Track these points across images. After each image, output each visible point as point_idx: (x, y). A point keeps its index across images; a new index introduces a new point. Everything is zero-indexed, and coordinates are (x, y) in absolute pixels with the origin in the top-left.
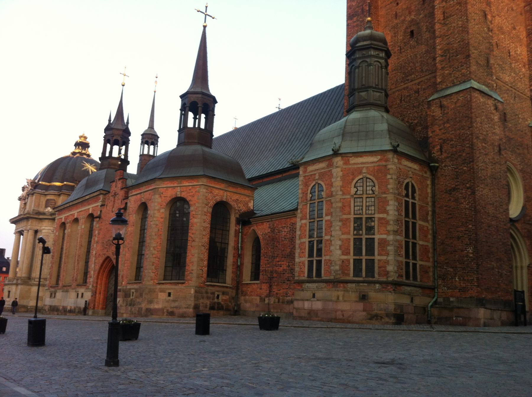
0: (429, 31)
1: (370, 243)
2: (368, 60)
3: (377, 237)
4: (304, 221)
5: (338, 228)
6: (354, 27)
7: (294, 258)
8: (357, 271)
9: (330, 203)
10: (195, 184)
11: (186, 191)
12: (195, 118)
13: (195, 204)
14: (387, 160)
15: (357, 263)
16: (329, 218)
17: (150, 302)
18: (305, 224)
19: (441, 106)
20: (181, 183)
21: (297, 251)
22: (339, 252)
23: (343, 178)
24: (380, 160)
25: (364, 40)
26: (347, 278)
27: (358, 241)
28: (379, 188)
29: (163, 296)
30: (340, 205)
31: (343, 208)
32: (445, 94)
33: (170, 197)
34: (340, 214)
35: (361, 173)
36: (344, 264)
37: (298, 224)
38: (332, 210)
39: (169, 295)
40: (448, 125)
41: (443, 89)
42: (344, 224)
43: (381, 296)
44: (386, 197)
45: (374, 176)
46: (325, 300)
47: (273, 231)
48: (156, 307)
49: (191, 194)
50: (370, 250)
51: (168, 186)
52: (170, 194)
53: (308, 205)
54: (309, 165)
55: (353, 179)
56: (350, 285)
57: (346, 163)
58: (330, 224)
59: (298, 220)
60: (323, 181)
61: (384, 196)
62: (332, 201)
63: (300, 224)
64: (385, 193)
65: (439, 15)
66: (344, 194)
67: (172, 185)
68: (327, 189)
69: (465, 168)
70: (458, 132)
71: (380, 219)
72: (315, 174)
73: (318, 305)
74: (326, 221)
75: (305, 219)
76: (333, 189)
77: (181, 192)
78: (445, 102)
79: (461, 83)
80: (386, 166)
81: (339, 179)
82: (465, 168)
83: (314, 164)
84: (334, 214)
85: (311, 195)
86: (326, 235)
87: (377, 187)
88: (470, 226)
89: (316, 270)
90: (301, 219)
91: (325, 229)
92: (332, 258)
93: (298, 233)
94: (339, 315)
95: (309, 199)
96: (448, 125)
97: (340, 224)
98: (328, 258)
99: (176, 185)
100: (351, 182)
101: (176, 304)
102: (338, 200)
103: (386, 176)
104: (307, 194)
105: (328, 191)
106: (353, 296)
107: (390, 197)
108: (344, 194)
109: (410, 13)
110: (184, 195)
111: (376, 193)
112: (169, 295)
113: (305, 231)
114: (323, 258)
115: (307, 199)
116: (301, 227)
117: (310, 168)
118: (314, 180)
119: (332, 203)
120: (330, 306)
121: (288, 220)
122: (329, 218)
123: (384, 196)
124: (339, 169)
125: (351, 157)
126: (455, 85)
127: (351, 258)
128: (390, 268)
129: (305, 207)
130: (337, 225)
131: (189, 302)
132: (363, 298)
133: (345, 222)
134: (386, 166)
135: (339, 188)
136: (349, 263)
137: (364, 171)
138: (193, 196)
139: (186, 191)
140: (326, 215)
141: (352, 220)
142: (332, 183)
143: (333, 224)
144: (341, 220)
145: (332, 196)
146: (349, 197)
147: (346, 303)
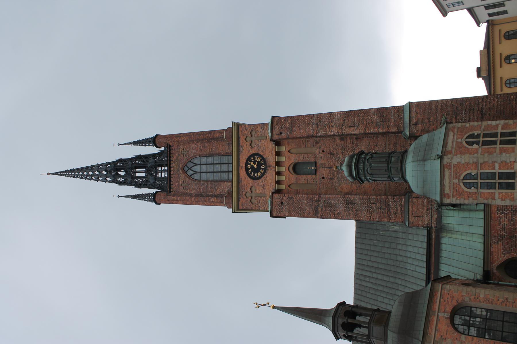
0: (355, 149)
4: (497, 196)
5: (508, 155)
6: (325, 210)
9: (484, 164)
10: (439, 295)
11: (445, 305)
12: (360, 326)
13: (462, 296)
16: (497, 165)
18: (500, 193)
19: (416, 124)
20: (435, 311)
24: (453, 131)
25: (352, 162)
28: (476, 131)
30: (486, 155)
31: (490, 153)
32: (408, 120)
33: (448, 326)
34: (495, 154)
35: (461, 143)
37: (498, 202)
38: (490, 162)
40: (432, 118)
41: (403, 126)
42: (505, 152)
44: (484, 126)
45: (465, 134)
47: (501, 238)
49: (450, 300)
51: (434, 328)
52: (444, 326)
53: (482, 191)
54: (444, 191)
55: (465, 147)
57: (450, 152)
58: (504, 164)
59: (494, 203)
60: (462, 174)
61: (483, 127)
62: (482, 162)
63: (499, 200)
64: (481, 127)
65: (350, 131)
66: (477, 153)
67: (435, 323)
68: (470, 169)
69: (467, 104)
70: (439, 110)
71: (502, 128)
72: (454, 183)
74: (500, 168)
75: (495, 195)
76: (471, 162)
77: (445, 312)
78: (414, 121)
79: (404, 113)
80: (458, 128)
81: (463, 156)
82: (467, 104)
83: (444, 185)
84: (495, 160)
85: (473, 188)
87: (474, 132)
88: (512, 97)
90: (494, 199)
91: (508, 169)
93: (507, 203)
95: (475, 190)
96: (432, 118)
97: (504, 154)
99: (435, 318)
100: (468, 148)
102: (482, 156)
103: (466, 128)
104: (470, 193)
105: (472, 168)
108: (477, 153)
110: (449, 309)
111: (480, 132)
113: (506, 193)
115: (476, 193)
116: (502, 200)
117: (447, 190)
118: (459, 184)
119: (484, 162)
121: (493, 215)
122: (497, 165)
123: (483, 127)
124: (455, 157)
125: (446, 150)
126: (403, 117)
129: (483, 195)
133: (502, 151)
134: (458, 128)
135: (471, 156)
137: (459, 140)
138: (453, 297)
139: (445, 305)
140: (494, 169)
141: (501, 146)
142: (466, 163)
143: (504, 159)
144: (501, 153)
145: (476, 163)
146: (480, 149)
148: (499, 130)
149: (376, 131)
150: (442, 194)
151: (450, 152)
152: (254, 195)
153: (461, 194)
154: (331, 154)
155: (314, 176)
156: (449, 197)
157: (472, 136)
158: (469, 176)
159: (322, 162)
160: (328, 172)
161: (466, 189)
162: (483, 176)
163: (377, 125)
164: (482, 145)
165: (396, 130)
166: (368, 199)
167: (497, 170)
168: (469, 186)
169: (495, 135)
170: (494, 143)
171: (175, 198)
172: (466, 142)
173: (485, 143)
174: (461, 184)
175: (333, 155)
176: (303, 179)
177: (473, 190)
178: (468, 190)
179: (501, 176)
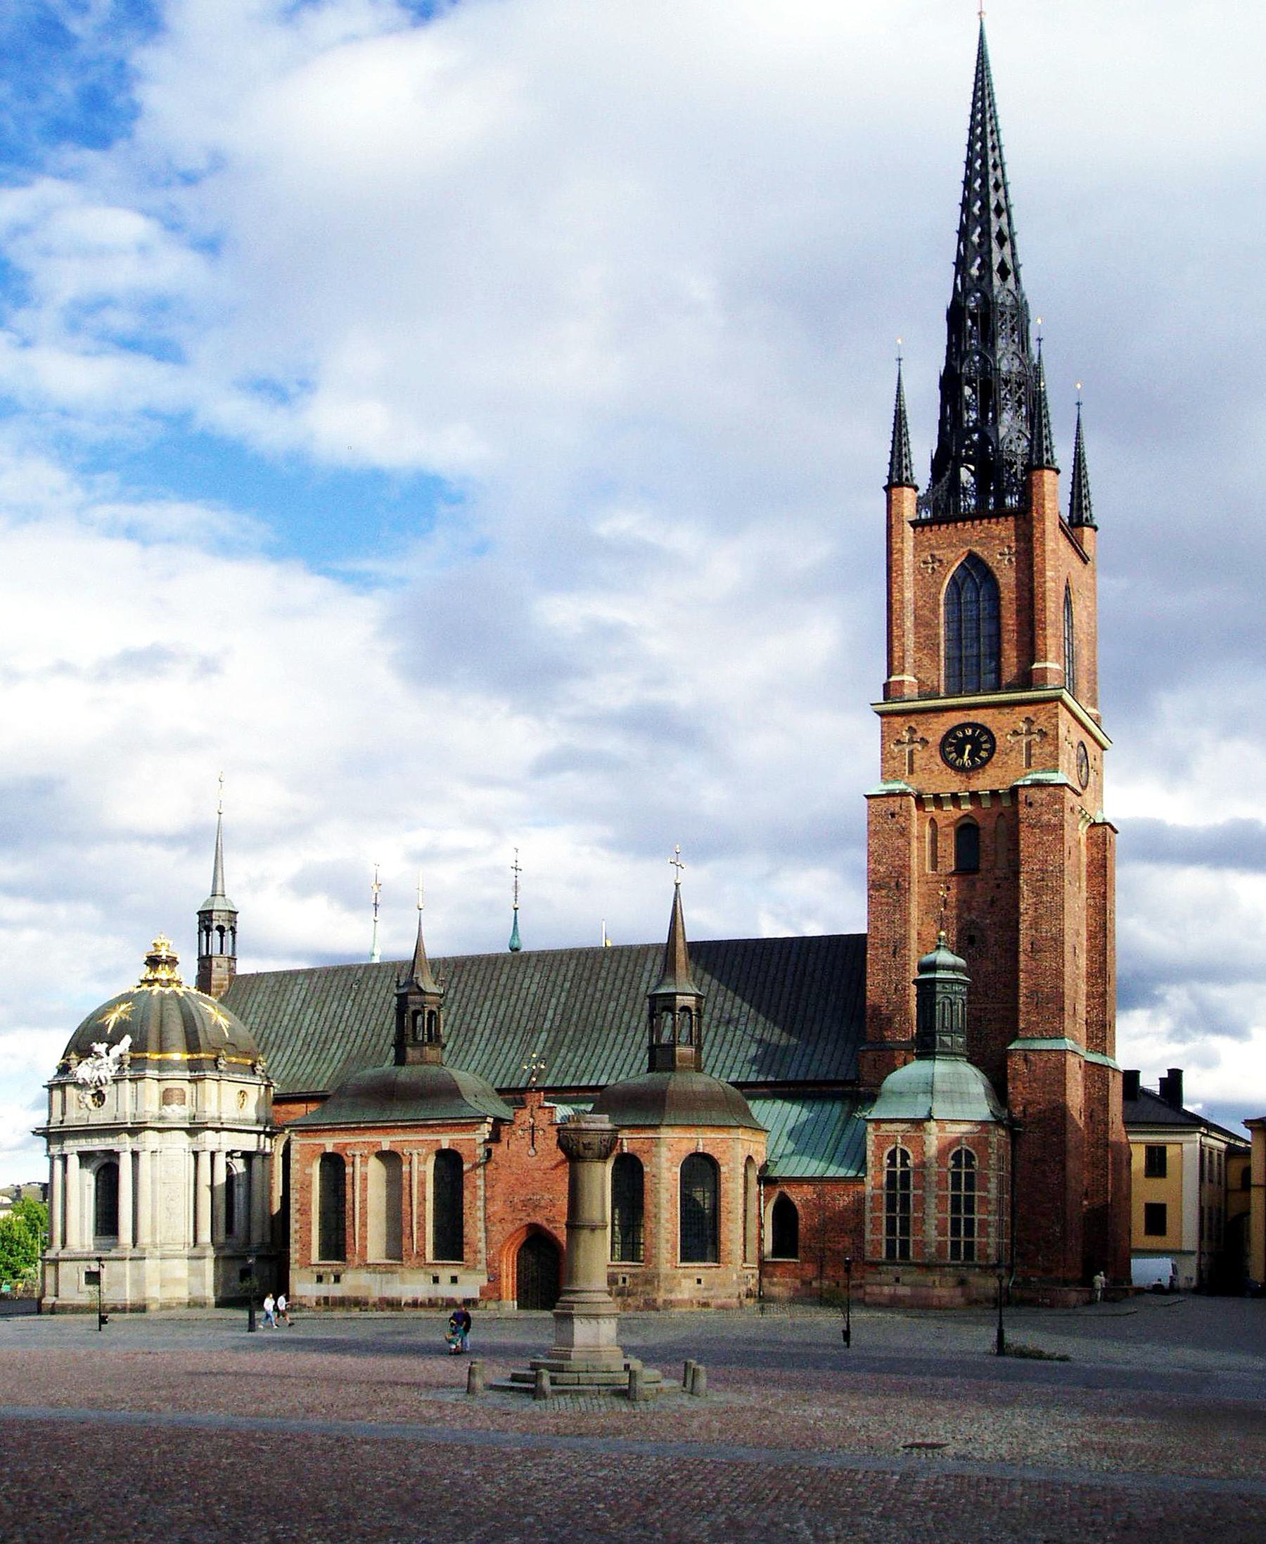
1: (970, 1223)
2: (952, 997)
3: (977, 1217)
5: (933, 1206)
7: (863, 1236)
8: (955, 1254)
14: (988, 1132)
15: (955, 1245)
16: (920, 1192)
17: (671, 1291)
21: (868, 1227)
22: (934, 1233)
26: (943, 1262)
27: (956, 1222)
29: (692, 1283)
30: (935, 1178)
31: (938, 1183)
36: (941, 1247)
39: (699, 1281)
43: (982, 1281)
46: (913, 1285)
48: (680, 1297)
50: (969, 1232)
56: (947, 1269)
57: (942, 1130)
58: (921, 1201)
73: (903, 1291)
80: (986, 1139)
86: (915, 1211)
89: (899, 1253)
92: (926, 1240)
94: (935, 1302)
98: (919, 1238)
101: (712, 1293)
106: (951, 1281)
107: (991, 1173)
112: (699, 1281)
114: (912, 1239)
117: (885, 1127)
120: (924, 1291)
122: (920, 1192)
127: (949, 1238)
128: (991, 1251)
131: (730, 1291)
132: (962, 1283)
133: (941, 1199)
147: (943, 1289)
149: (1023, 991)
150: (878, 1122)
151: (942, 1130)
153: (880, 1147)
154: (993, 902)
156: (875, 1130)
157: (970, 1156)
158: (905, 1155)
161: (886, 1154)
163: (1033, 993)
164: (953, 1173)
165: (1022, 1026)
167: (913, 1192)
168: (892, 1156)
169: (970, 1186)
170: (956, 1185)
172: (958, 1153)
173: (956, 1177)
174: (893, 1147)
175: (992, 906)
177: (886, 1161)
179: (905, 1198)
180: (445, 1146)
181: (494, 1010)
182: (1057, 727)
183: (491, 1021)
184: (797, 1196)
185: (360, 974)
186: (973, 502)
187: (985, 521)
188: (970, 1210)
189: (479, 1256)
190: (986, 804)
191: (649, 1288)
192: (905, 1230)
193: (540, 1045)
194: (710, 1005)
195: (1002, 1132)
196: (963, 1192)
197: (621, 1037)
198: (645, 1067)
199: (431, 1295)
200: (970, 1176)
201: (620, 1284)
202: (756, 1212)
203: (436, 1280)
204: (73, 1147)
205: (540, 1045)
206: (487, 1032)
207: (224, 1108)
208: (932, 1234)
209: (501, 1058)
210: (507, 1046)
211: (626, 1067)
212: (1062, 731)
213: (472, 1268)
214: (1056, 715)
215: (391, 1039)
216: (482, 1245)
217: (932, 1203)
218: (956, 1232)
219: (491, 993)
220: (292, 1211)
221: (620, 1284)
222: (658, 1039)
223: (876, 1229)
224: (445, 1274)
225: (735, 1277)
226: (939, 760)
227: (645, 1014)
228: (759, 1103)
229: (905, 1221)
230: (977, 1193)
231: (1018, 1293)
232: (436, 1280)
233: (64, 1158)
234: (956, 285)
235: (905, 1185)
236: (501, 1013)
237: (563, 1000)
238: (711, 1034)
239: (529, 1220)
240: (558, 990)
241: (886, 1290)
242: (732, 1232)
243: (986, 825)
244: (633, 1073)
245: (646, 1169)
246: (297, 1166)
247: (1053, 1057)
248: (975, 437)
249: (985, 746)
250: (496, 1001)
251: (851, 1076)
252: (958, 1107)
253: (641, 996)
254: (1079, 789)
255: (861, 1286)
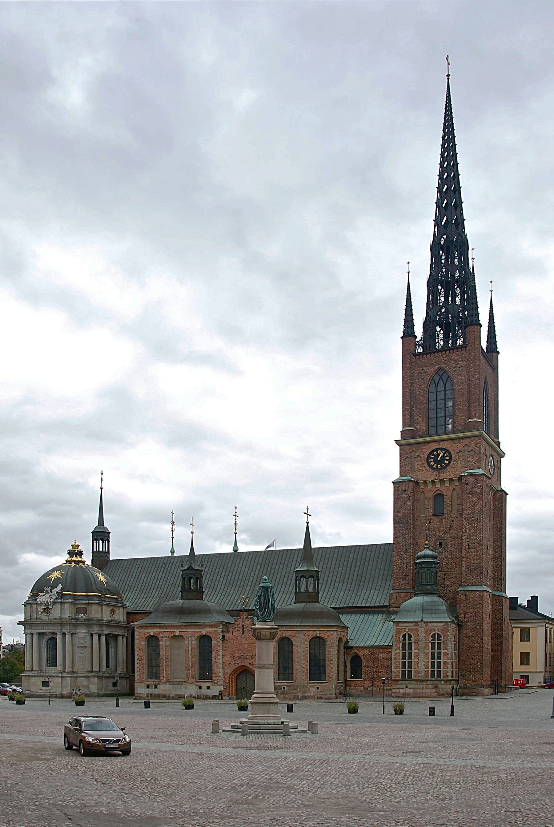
16: (417, 651)
17: (305, 692)
23: (425, 633)
31: (425, 647)
50: (439, 667)
53: (401, 644)
66: (425, 640)
107: (449, 643)
108: (425, 640)
109: (439, 532)
122: (417, 651)
130: (422, 655)
133: (426, 654)
136: (428, 673)
137: (436, 630)
145: (418, 640)
148: (442, 651)
152: (413, 459)
155: (431, 514)
157: (439, 636)
158: (410, 636)
159: (444, 520)
160: (435, 526)
162: (410, 644)
166: (410, 562)
167: (413, 651)
168: (404, 636)
169: (439, 648)
171: (408, 365)
176: (430, 504)
177: (402, 639)
178: (401, 636)
180: (204, 634)
181: (226, 577)
182: (480, 448)
183: (224, 581)
184: (361, 654)
185: (165, 561)
186: (442, 343)
187: (448, 352)
188: (439, 658)
189: (219, 678)
190: (447, 484)
191: (295, 691)
192: (410, 667)
193: (247, 592)
194: (323, 575)
195: (454, 626)
196: (436, 651)
197: (283, 588)
198: (294, 601)
199: (199, 694)
200: (439, 644)
201: (283, 689)
202: (343, 660)
203: (200, 688)
204: (36, 630)
205: (247, 592)
206: (223, 586)
207: (104, 616)
208: (422, 668)
209: (229, 597)
210: (232, 592)
211: (285, 601)
212: (482, 450)
213: (217, 684)
214: (480, 443)
215: (180, 589)
216: (221, 674)
217: (422, 655)
218: (433, 666)
219: (224, 570)
220: (136, 659)
221: (283, 689)
222: (300, 589)
223: (398, 666)
224: (204, 685)
225: (334, 687)
226: (426, 465)
227: (294, 578)
228: (345, 616)
229: (410, 663)
230: (442, 651)
231: (461, 691)
232: (200, 688)
233: (32, 634)
234: (435, 232)
235: (410, 648)
236: (229, 578)
237: (257, 573)
238: (323, 587)
239: (241, 664)
240: (254, 568)
241: (401, 691)
242: (332, 669)
243: (447, 493)
244: (288, 603)
245: (294, 643)
246: (138, 641)
247: (477, 593)
248: (443, 310)
249: (447, 458)
250: (227, 573)
251: (386, 604)
252: (434, 616)
253: (292, 571)
254: (490, 476)
255: (390, 689)
